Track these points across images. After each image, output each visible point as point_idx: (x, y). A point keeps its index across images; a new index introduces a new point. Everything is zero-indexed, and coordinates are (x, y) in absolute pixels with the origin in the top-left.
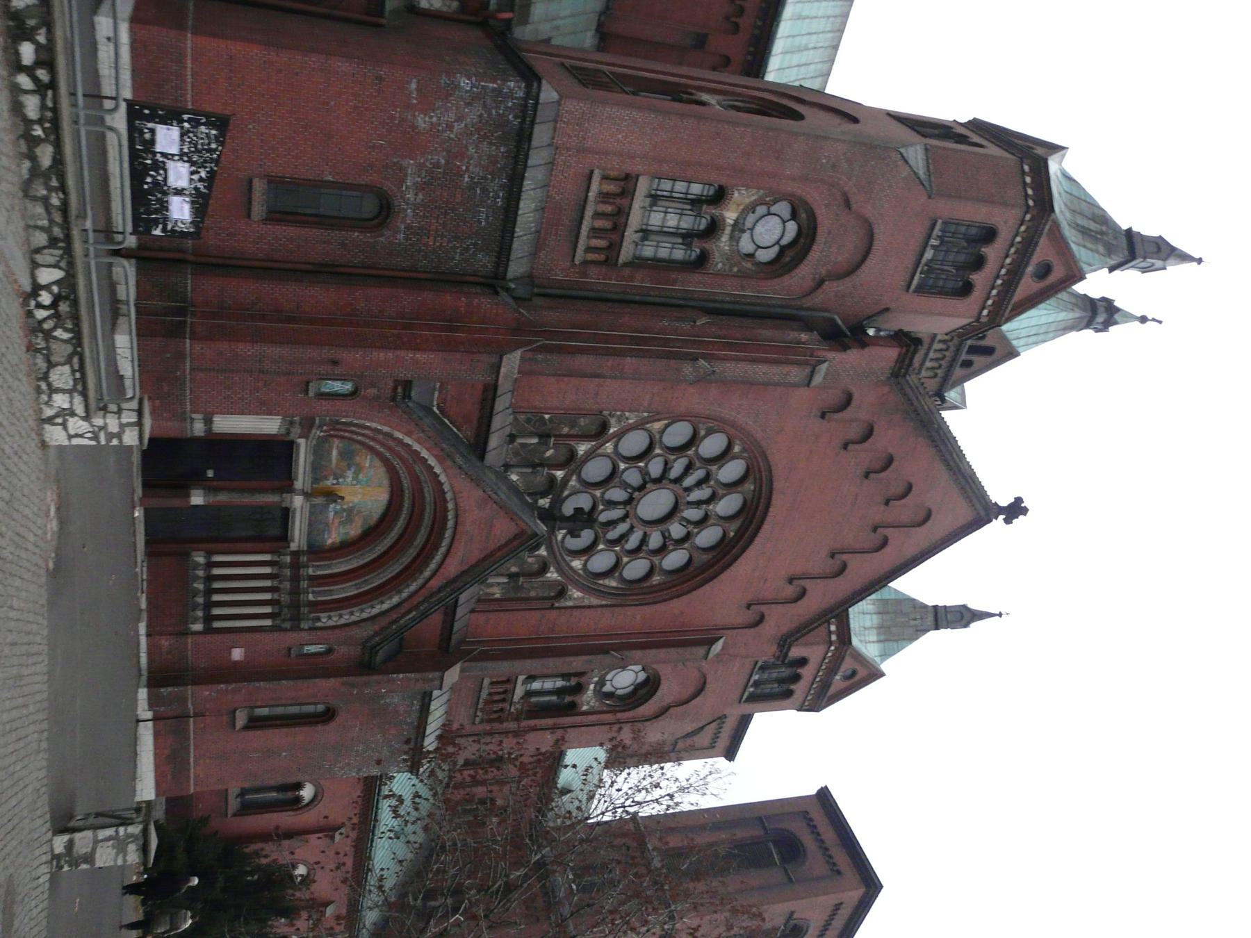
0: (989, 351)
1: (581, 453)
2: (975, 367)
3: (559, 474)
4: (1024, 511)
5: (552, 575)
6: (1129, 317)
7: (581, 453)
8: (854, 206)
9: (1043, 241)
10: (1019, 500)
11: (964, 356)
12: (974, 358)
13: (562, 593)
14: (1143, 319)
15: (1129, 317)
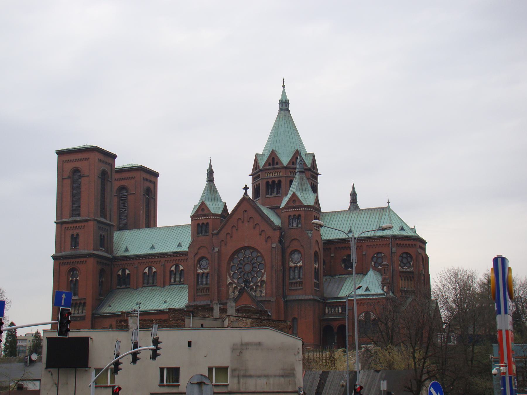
0: (273, 158)
1: (235, 285)
2: (278, 161)
3: (239, 288)
4: (246, 186)
5: (259, 284)
6: (284, 92)
7: (235, 285)
8: (196, 252)
9: (198, 214)
10: (243, 189)
11: (276, 166)
12: (275, 162)
13: (263, 281)
14: (284, 86)
15: (284, 92)
